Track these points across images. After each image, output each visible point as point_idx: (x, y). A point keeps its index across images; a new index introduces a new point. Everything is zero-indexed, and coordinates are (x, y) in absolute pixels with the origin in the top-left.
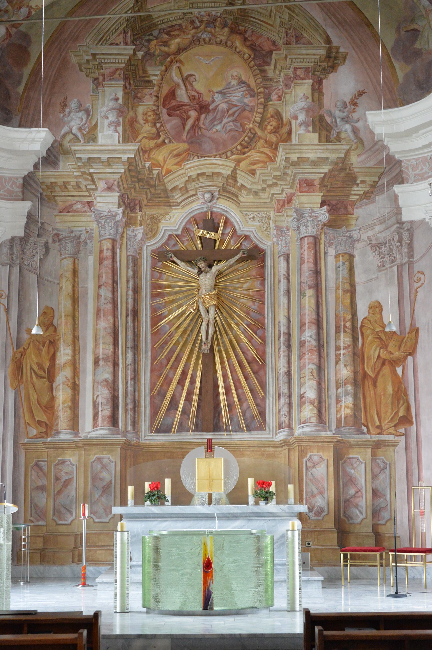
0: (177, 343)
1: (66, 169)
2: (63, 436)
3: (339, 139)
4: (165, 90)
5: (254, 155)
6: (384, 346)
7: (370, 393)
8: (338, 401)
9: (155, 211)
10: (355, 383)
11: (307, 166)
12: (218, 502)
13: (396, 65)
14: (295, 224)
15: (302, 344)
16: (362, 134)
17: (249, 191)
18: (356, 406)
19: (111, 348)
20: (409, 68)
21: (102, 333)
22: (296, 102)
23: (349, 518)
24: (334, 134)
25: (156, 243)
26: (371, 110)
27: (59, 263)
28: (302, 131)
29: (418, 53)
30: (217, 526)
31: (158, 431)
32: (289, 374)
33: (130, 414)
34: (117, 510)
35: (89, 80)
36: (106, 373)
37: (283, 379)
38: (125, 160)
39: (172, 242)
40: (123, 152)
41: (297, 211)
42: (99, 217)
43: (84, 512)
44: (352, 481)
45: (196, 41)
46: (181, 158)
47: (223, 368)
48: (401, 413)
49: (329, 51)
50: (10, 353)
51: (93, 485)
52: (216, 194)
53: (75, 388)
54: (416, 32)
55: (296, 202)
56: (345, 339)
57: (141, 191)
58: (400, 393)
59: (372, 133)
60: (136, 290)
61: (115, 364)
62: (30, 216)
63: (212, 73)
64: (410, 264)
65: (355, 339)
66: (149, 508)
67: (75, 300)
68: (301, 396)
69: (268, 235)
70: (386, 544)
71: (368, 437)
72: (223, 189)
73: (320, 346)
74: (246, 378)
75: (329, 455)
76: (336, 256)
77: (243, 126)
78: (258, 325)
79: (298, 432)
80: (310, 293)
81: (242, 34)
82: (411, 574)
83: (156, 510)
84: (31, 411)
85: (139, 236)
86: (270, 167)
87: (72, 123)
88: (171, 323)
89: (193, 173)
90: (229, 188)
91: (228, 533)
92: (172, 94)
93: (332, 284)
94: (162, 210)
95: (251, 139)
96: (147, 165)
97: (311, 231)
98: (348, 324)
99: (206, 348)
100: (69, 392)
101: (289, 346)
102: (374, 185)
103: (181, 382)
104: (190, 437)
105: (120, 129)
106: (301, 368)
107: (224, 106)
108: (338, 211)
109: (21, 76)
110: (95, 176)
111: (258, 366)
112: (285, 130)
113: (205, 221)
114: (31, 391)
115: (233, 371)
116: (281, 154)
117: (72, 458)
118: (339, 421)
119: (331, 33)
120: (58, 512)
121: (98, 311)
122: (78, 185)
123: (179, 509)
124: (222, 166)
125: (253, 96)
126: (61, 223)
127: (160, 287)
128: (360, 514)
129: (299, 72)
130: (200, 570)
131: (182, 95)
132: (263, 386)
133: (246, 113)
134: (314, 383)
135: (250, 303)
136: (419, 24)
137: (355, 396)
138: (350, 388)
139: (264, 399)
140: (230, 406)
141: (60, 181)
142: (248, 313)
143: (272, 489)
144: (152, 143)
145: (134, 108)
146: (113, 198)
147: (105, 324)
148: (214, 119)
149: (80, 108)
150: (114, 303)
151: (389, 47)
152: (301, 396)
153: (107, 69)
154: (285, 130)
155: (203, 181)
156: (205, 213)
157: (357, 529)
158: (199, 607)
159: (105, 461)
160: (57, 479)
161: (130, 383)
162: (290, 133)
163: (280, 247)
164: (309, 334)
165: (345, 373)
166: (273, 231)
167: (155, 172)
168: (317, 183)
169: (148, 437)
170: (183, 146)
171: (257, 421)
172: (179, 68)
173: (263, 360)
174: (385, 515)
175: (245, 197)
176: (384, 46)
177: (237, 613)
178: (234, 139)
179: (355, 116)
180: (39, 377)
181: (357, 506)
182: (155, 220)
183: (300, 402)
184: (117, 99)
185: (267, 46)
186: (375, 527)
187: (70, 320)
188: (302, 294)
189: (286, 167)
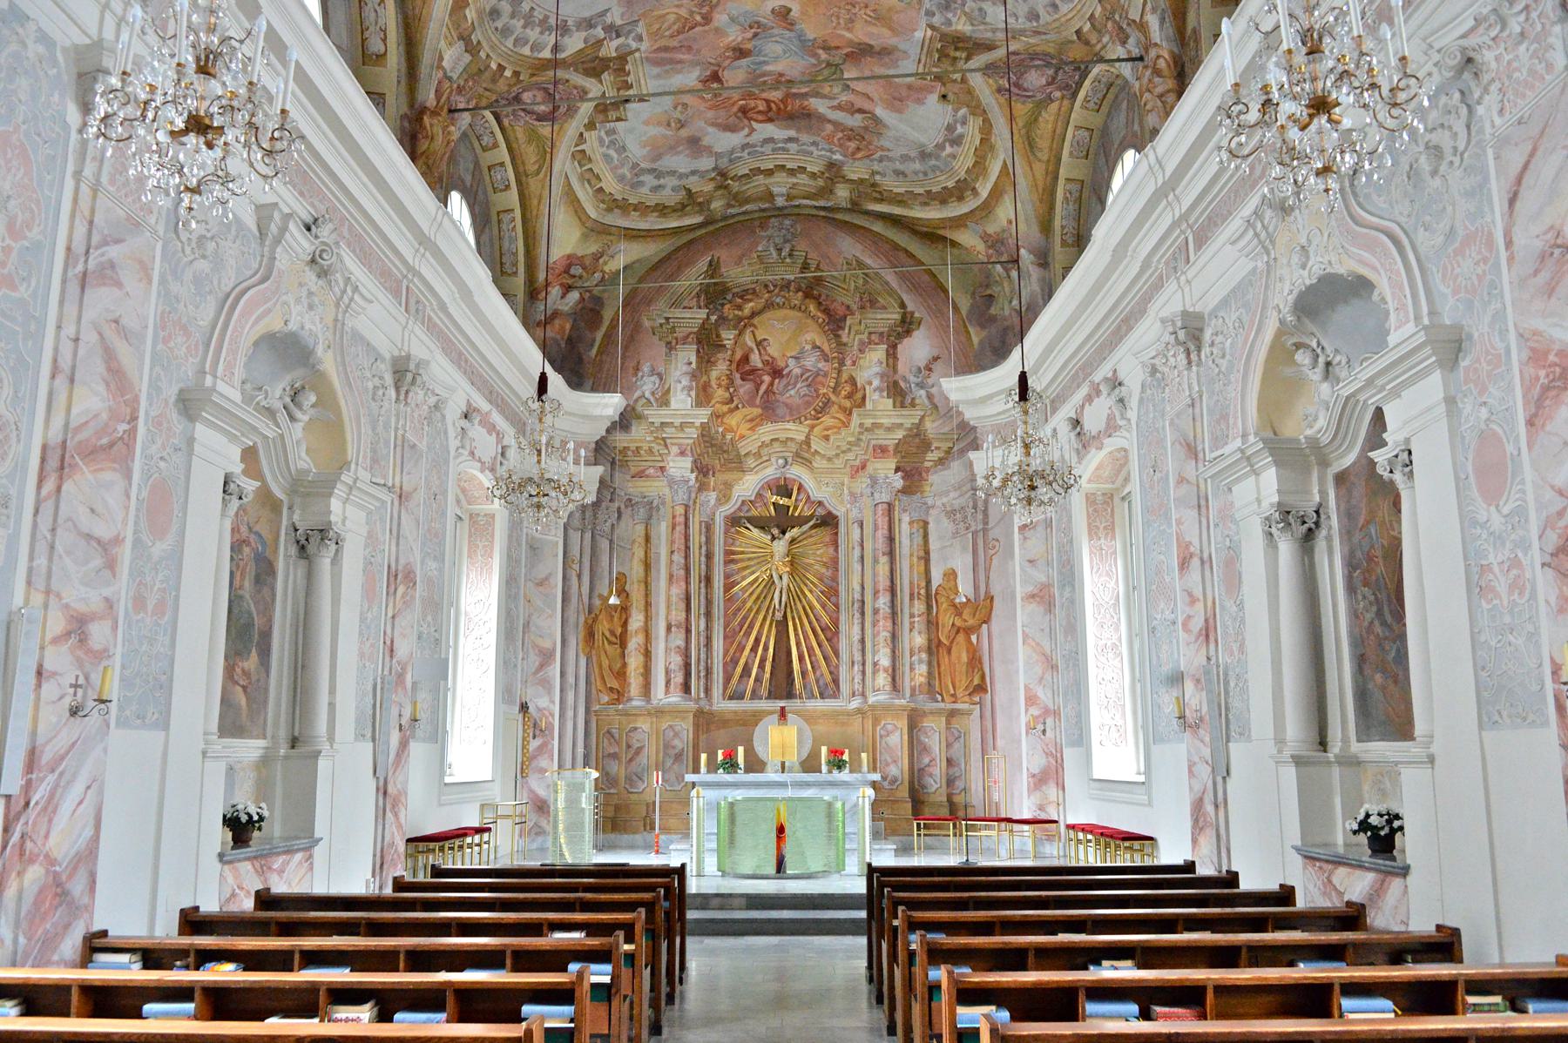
0: (750, 610)
2: (635, 703)
3: (913, 405)
4: (738, 356)
5: (827, 420)
6: (959, 614)
7: (945, 660)
8: (912, 669)
9: (728, 476)
10: (929, 650)
11: (881, 432)
12: (791, 771)
13: (971, 330)
14: (869, 490)
15: (876, 611)
18: (930, 673)
19: (684, 615)
20: (984, 333)
21: (674, 599)
22: (870, 367)
23: (923, 787)
25: (728, 509)
26: (946, 376)
27: (631, 529)
28: (876, 396)
29: (993, 319)
30: (789, 793)
31: (731, 698)
32: (863, 641)
33: (702, 681)
34: (690, 777)
36: (678, 640)
37: (857, 646)
39: (745, 508)
40: (696, 416)
41: (871, 477)
42: (672, 483)
43: (657, 778)
44: (925, 749)
45: (769, 306)
46: (755, 423)
47: (796, 635)
48: (976, 682)
49: (904, 316)
50: (582, 619)
51: (666, 754)
53: (647, 654)
54: (991, 298)
55: (870, 468)
56: (919, 607)
57: (714, 458)
58: (975, 661)
59: (947, 399)
60: (709, 556)
61: (688, 631)
62: (602, 481)
63: (786, 337)
64: (985, 531)
65: (929, 607)
66: (722, 776)
67: (647, 566)
68: (875, 664)
69: (842, 502)
70: (961, 814)
71: (942, 705)
72: (797, 455)
73: (894, 614)
74: (820, 646)
75: (903, 724)
76: (911, 523)
78: (832, 592)
79: (871, 700)
80: (884, 560)
81: (817, 299)
82: (986, 844)
83: (729, 778)
84: (603, 678)
85: (713, 502)
86: (844, 432)
88: (744, 590)
89: (767, 439)
90: (803, 454)
91: (801, 799)
92: (746, 359)
93: (906, 550)
94: (735, 475)
95: (825, 404)
97: (885, 497)
98: (923, 592)
99: (779, 616)
100: (641, 658)
101: (863, 614)
102: (949, 451)
103: (754, 649)
104: (764, 705)
105: (693, 393)
106: (874, 636)
107: (797, 371)
108: (913, 478)
109: (594, 340)
111: (831, 634)
112: (859, 395)
113: (779, 487)
114: (603, 657)
115: (806, 638)
116: (855, 420)
117: (644, 725)
118: (913, 690)
119: (906, 298)
120: (629, 779)
121: (671, 576)
122: (650, 449)
123: (752, 777)
124: (796, 431)
126: (636, 488)
127: (734, 553)
128: (935, 784)
129: (873, 337)
130: (774, 835)
131: (756, 360)
132: (837, 654)
133: (820, 378)
134: (888, 651)
135: (823, 570)
136: (995, 290)
137: (930, 664)
138: (924, 656)
139: (837, 667)
140: (804, 673)
141: (633, 446)
142: (821, 580)
143: (846, 757)
144: (725, 408)
145: (707, 372)
146: (687, 463)
147: (677, 590)
149: (653, 372)
150: (687, 569)
151: (964, 313)
152: (875, 664)
153: (680, 333)
154: (859, 395)
155: (777, 447)
157: (932, 799)
158: (772, 870)
159: (678, 728)
160: (629, 746)
161: (703, 650)
162: (864, 398)
163: (854, 514)
164: (883, 601)
165: (920, 640)
166: (847, 497)
167: (729, 437)
169: (721, 704)
170: (757, 411)
171: (831, 689)
173: (836, 625)
174: (960, 784)
175: (818, 463)
177: (809, 876)
178: (808, 404)
179: (930, 381)
180: (610, 643)
181: (931, 775)
182: (728, 486)
183: (873, 671)
185: (841, 311)
186: (950, 796)
187: (642, 586)
188: (876, 561)
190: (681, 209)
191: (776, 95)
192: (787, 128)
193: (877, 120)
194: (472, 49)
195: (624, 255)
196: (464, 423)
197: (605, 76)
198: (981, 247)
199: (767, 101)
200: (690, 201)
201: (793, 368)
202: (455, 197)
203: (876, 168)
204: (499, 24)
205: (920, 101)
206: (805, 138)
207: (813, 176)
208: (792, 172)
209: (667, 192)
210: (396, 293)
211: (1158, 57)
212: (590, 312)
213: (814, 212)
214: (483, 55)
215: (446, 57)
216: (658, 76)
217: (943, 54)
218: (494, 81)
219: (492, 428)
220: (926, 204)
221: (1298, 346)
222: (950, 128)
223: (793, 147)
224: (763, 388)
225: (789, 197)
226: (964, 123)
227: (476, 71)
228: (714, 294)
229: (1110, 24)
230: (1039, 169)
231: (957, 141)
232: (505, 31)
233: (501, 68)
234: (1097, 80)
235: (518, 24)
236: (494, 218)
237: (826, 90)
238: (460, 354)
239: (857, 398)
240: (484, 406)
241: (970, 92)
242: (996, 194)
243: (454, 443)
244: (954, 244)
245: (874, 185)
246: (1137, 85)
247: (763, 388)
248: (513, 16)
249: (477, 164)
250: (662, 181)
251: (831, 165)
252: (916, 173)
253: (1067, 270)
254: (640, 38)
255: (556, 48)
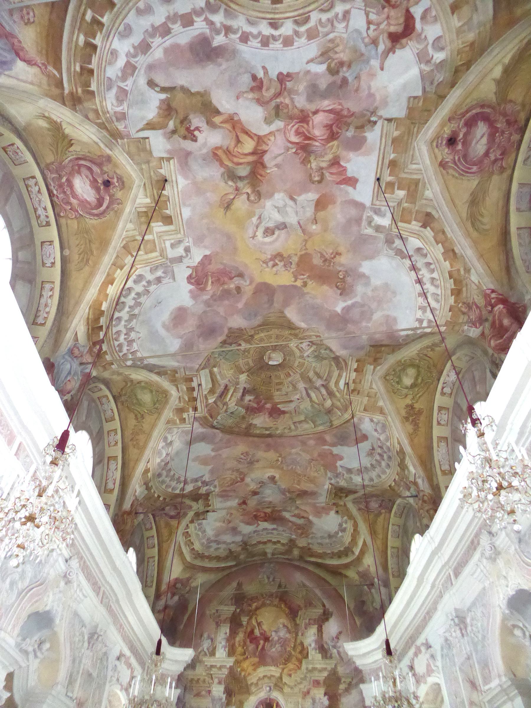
1: (200, 671)
3: (331, 657)
4: (249, 629)
5: (291, 666)
13: (356, 618)
16: (342, 654)
17: (289, 686)
22: (310, 637)
24: (329, 655)
26: (346, 642)
28: (313, 652)
35: (214, 623)
38: (228, 666)
45: (264, 605)
46: (256, 666)
52: (272, 688)
55: (312, 693)
59: (347, 654)
63: (271, 622)
72: (276, 685)
77: (285, 649)
86: (299, 672)
87: (204, 646)
89: (261, 675)
90: (279, 685)
92: (252, 632)
96: (239, 670)
102: (350, 684)
105: (227, 649)
107: (276, 638)
110: (213, 676)
116: (304, 666)
122: (204, 681)
125: (290, 633)
131: (257, 632)
136: (365, 598)
141: (196, 679)
145: (234, 638)
146: (222, 688)
148: (271, 646)
149: (209, 637)
153: (223, 618)
154: (305, 652)
155: (266, 680)
156: (266, 699)
167: (243, 674)
168: (322, 682)
172: (256, 618)
175: (286, 690)
176: (349, 608)
179: (338, 644)
184: (226, 633)
189: (307, 673)
190: (226, 558)
191: (268, 510)
192: (273, 524)
193: (310, 522)
194: (148, 488)
195: (200, 579)
196: (117, 663)
197: (200, 501)
198: (356, 577)
199: (265, 513)
200: (231, 555)
201: (274, 637)
202: (131, 550)
203: (310, 541)
204: (161, 479)
205: (328, 514)
206: (281, 528)
207: (283, 545)
208: (275, 543)
209: (221, 550)
210: (98, 594)
211: (424, 495)
212: (183, 606)
213: (285, 561)
214: (152, 491)
215: (138, 491)
216: (221, 502)
217: (336, 495)
218: (155, 502)
219: (129, 666)
220: (332, 558)
221: (514, 626)
222: (340, 525)
223: (274, 532)
224: (260, 647)
225: (273, 554)
226: (346, 523)
227: (149, 498)
228: (239, 599)
229: (402, 483)
230: (379, 542)
231: (344, 530)
232: (163, 482)
233: (159, 497)
234: (399, 505)
235: (168, 480)
236: (146, 559)
237: (289, 509)
238: (121, 625)
239: (304, 653)
240: (128, 653)
241: (348, 510)
242: (363, 552)
243: (110, 673)
244: (346, 576)
245: (309, 549)
246: (417, 507)
247: (260, 647)
248: (167, 476)
249: (143, 535)
250: (220, 546)
251: (291, 541)
252: (327, 544)
253: (397, 589)
254: (215, 487)
255: (183, 489)
